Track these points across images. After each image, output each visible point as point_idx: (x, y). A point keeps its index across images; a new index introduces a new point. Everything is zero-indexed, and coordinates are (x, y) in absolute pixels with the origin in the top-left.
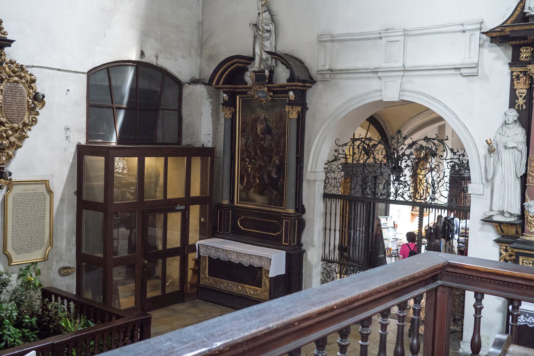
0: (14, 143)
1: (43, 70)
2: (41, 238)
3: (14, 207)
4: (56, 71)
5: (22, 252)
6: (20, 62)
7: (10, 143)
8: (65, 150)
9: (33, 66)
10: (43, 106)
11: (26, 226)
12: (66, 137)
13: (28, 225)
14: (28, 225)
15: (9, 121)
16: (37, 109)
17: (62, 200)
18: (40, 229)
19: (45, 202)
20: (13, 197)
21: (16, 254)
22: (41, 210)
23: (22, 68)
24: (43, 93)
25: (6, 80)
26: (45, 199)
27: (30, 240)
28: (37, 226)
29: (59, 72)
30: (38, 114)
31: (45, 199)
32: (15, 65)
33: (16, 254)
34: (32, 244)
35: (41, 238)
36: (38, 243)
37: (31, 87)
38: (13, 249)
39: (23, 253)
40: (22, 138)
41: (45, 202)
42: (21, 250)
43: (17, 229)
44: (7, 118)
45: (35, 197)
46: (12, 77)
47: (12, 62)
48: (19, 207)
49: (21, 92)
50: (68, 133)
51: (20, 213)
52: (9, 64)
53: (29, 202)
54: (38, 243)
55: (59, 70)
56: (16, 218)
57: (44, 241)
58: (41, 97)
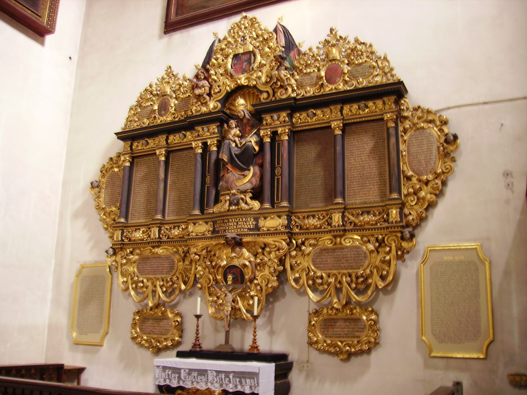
0: (424, 198)
1: (463, 109)
4: (481, 107)
6: (425, 105)
7: (418, 199)
8: (507, 202)
9: (448, 108)
10: (457, 147)
12: (507, 185)
15: (416, 173)
16: (452, 155)
17: (507, 273)
23: (429, 112)
24: (454, 133)
25: (410, 130)
29: (486, 107)
30: (453, 160)
32: (420, 111)
37: (441, 130)
38: (434, 336)
40: (439, 194)
44: (413, 171)
46: (418, 123)
47: (416, 109)
49: (428, 139)
50: (509, 180)
52: (414, 112)
55: (485, 103)
58: (452, 138)
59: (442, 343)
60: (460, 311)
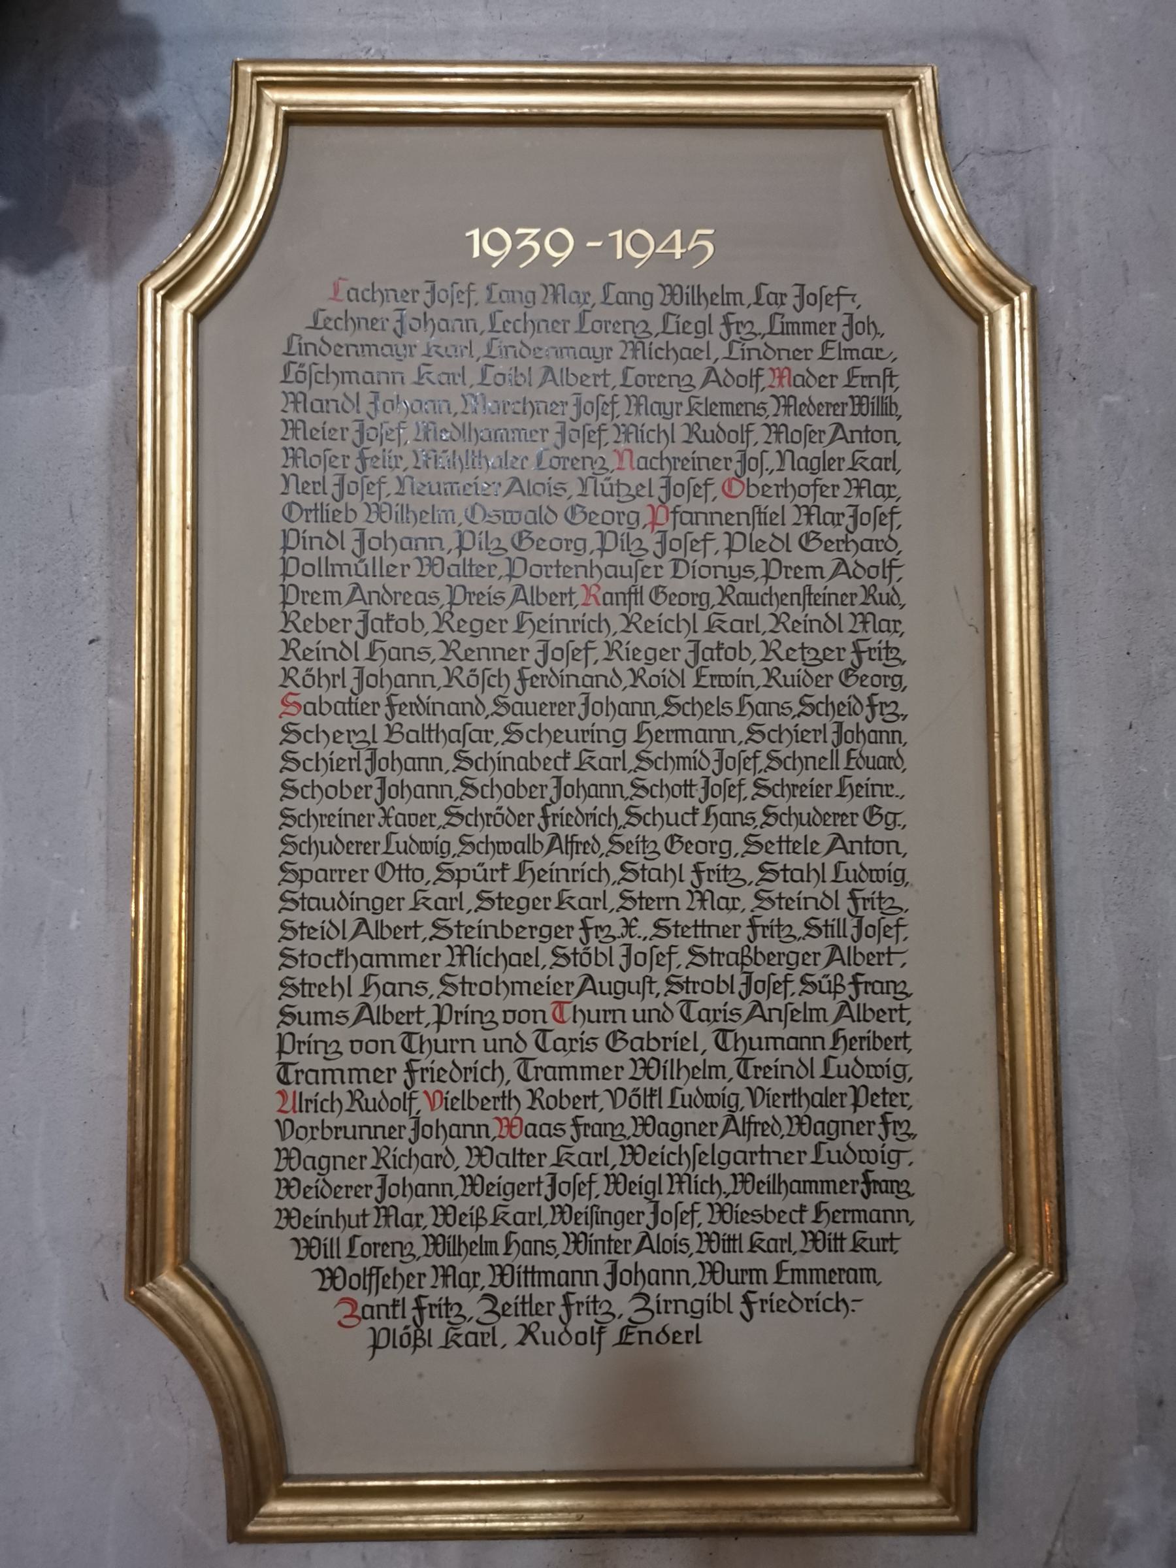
2: (827, 1099)
3: (320, 513)
5: (472, 1303)
11: (527, 846)
13: (572, 846)
14: (572, 846)
18: (796, 918)
19: (888, 463)
20: (293, 346)
21: (362, 1333)
22: (808, 597)
26: (886, 407)
27: (624, 1115)
28: (749, 867)
31: (886, 407)
33: (362, 1333)
34: (650, 1191)
35: (827, 1099)
36: (775, 1185)
39: (484, 1339)
41: (888, 463)
42: (445, 1274)
43: (371, 888)
45: (698, 370)
48: (403, 514)
51: (413, 624)
53: (573, 450)
54: (775, 1185)
56: (351, 707)
57: (893, 1158)
59: (417, 1340)
60: (646, 922)
